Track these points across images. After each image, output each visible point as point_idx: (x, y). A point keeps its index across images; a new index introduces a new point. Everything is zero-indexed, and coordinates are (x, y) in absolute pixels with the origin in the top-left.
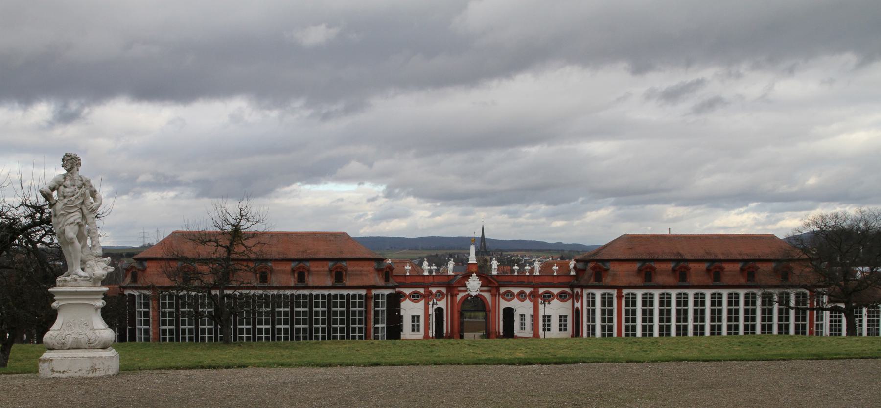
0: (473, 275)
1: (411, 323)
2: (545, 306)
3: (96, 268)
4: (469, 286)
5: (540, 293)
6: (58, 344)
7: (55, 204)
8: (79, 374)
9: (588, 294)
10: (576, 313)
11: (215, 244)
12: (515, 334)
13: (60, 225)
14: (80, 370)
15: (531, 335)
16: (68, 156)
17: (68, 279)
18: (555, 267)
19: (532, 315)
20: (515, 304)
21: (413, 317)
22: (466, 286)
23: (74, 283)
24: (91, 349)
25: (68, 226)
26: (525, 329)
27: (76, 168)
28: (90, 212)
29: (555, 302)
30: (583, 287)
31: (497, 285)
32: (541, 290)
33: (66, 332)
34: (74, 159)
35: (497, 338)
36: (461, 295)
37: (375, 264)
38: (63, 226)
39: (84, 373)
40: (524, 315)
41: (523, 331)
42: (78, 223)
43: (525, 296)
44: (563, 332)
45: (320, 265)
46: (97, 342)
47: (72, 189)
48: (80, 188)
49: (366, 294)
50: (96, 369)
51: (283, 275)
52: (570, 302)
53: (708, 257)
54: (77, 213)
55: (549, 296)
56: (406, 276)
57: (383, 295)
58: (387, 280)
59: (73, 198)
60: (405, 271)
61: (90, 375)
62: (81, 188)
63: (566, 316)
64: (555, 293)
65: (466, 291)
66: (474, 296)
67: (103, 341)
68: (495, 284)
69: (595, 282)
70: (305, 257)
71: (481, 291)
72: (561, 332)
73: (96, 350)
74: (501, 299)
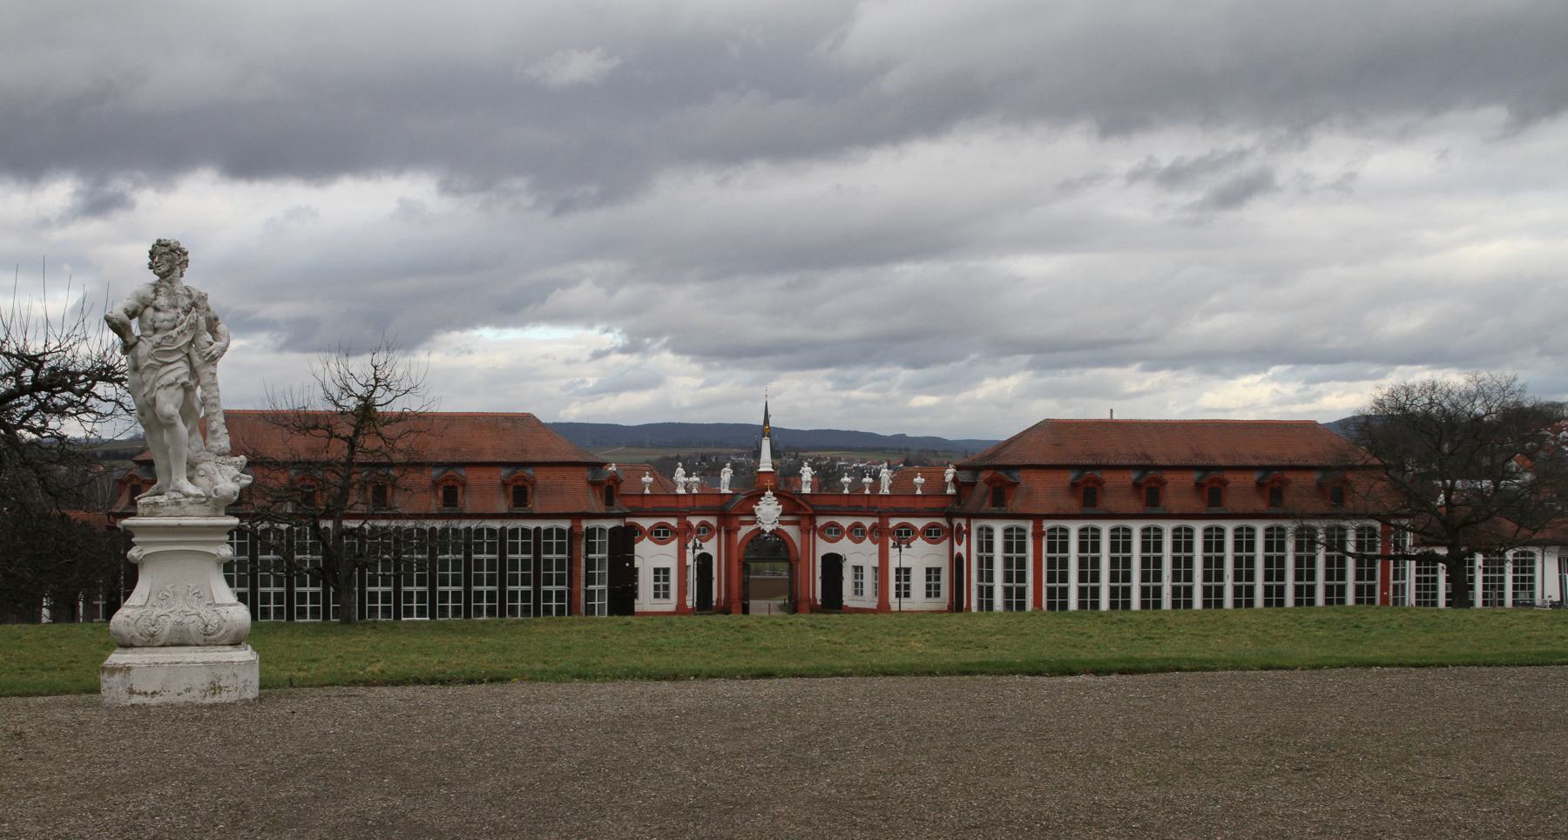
0: (766, 493)
2: (900, 551)
3: (219, 478)
4: (759, 514)
5: (890, 526)
6: (141, 634)
7: (135, 344)
8: (187, 697)
9: (980, 529)
10: (957, 564)
11: (325, 433)
12: (845, 603)
13: (146, 389)
14: (188, 690)
15: (874, 605)
16: (163, 245)
17: (162, 499)
18: (919, 480)
19: (875, 569)
20: (844, 547)
21: (657, 571)
22: (755, 515)
23: (174, 508)
24: (209, 645)
25: (162, 390)
26: (862, 594)
27: (178, 271)
28: (207, 361)
29: (919, 544)
30: (970, 517)
31: (811, 512)
32: (894, 522)
33: (158, 611)
34: (174, 251)
36: (744, 531)
37: (587, 473)
38: (152, 390)
39: (196, 697)
40: (862, 568)
41: (860, 598)
42: (183, 384)
43: (863, 532)
44: (932, 599)
45: (485, 474)
46: (222, 632)
47: (171, 314)
48: (187, 312)
49: (571, 530)
50: (220, 687)
51: (485, 493)
52: (946, 543)
53: (1200, 462)
54: (181, 364)
55: (907, 533)
56: (643, 495)
57: (602, 530)
58: (609, 501)
59: (174, 333)
60: (643, 485)
61: (209, 700)
62: (189, 312)
63: (938, 570)
64: (919, 528)
65: (754, 522)
66: (768, 531)
67: (235, 629)
68: (806, 510)
69: (994, 506)
70: (457, 459)
72: (930, 600)
73: (219, 648)
74: (817, 535)
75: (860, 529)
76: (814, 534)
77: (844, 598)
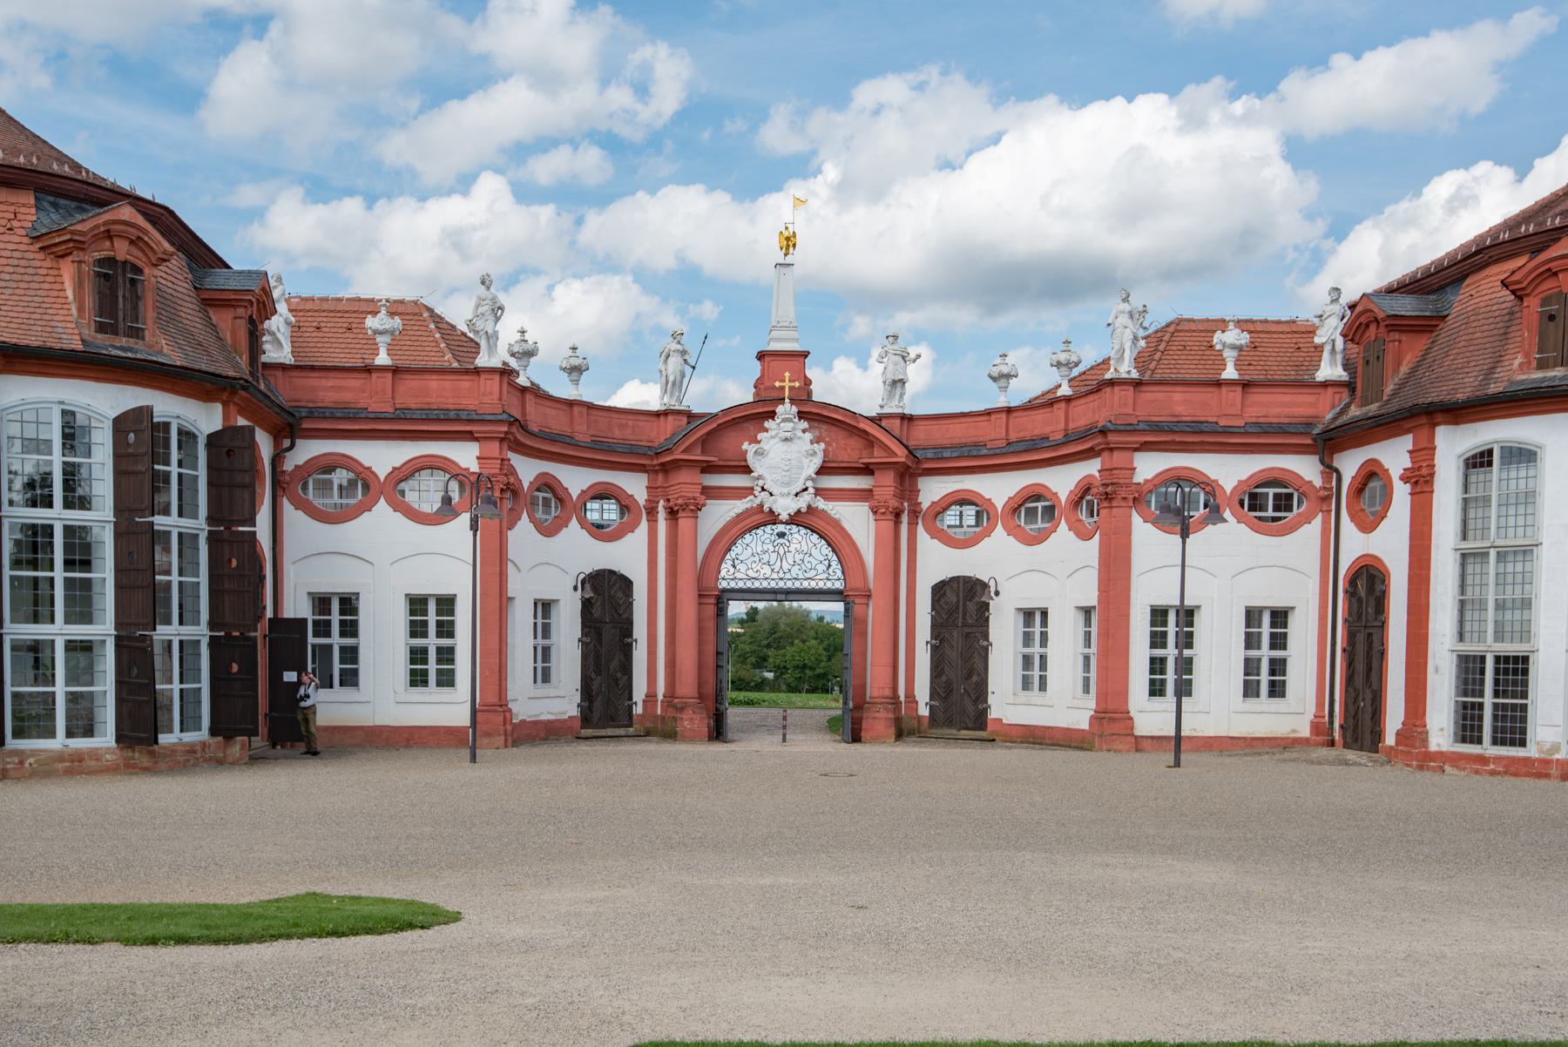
0: (780, 409)
1: (366, 641)
9: (1480, 460)
12: (993, 714)
19: (1087, 611)
21: (417, 604)
22: (747, 470)
26: (1043, 686)
32: (1148, 466)
35: (900, 735)
40: (1044, 613)
43: (1050, 511)
44: (1264, 702)
63: (1280, 617)
64: (1228, 484)
65: (748, 491)
69: (1542, 365)
71: (819, 492)
72: (1252, 703)
74: (920, 528)
75: (1040, 505)
76: (913, 524)
77: (991, 700)
